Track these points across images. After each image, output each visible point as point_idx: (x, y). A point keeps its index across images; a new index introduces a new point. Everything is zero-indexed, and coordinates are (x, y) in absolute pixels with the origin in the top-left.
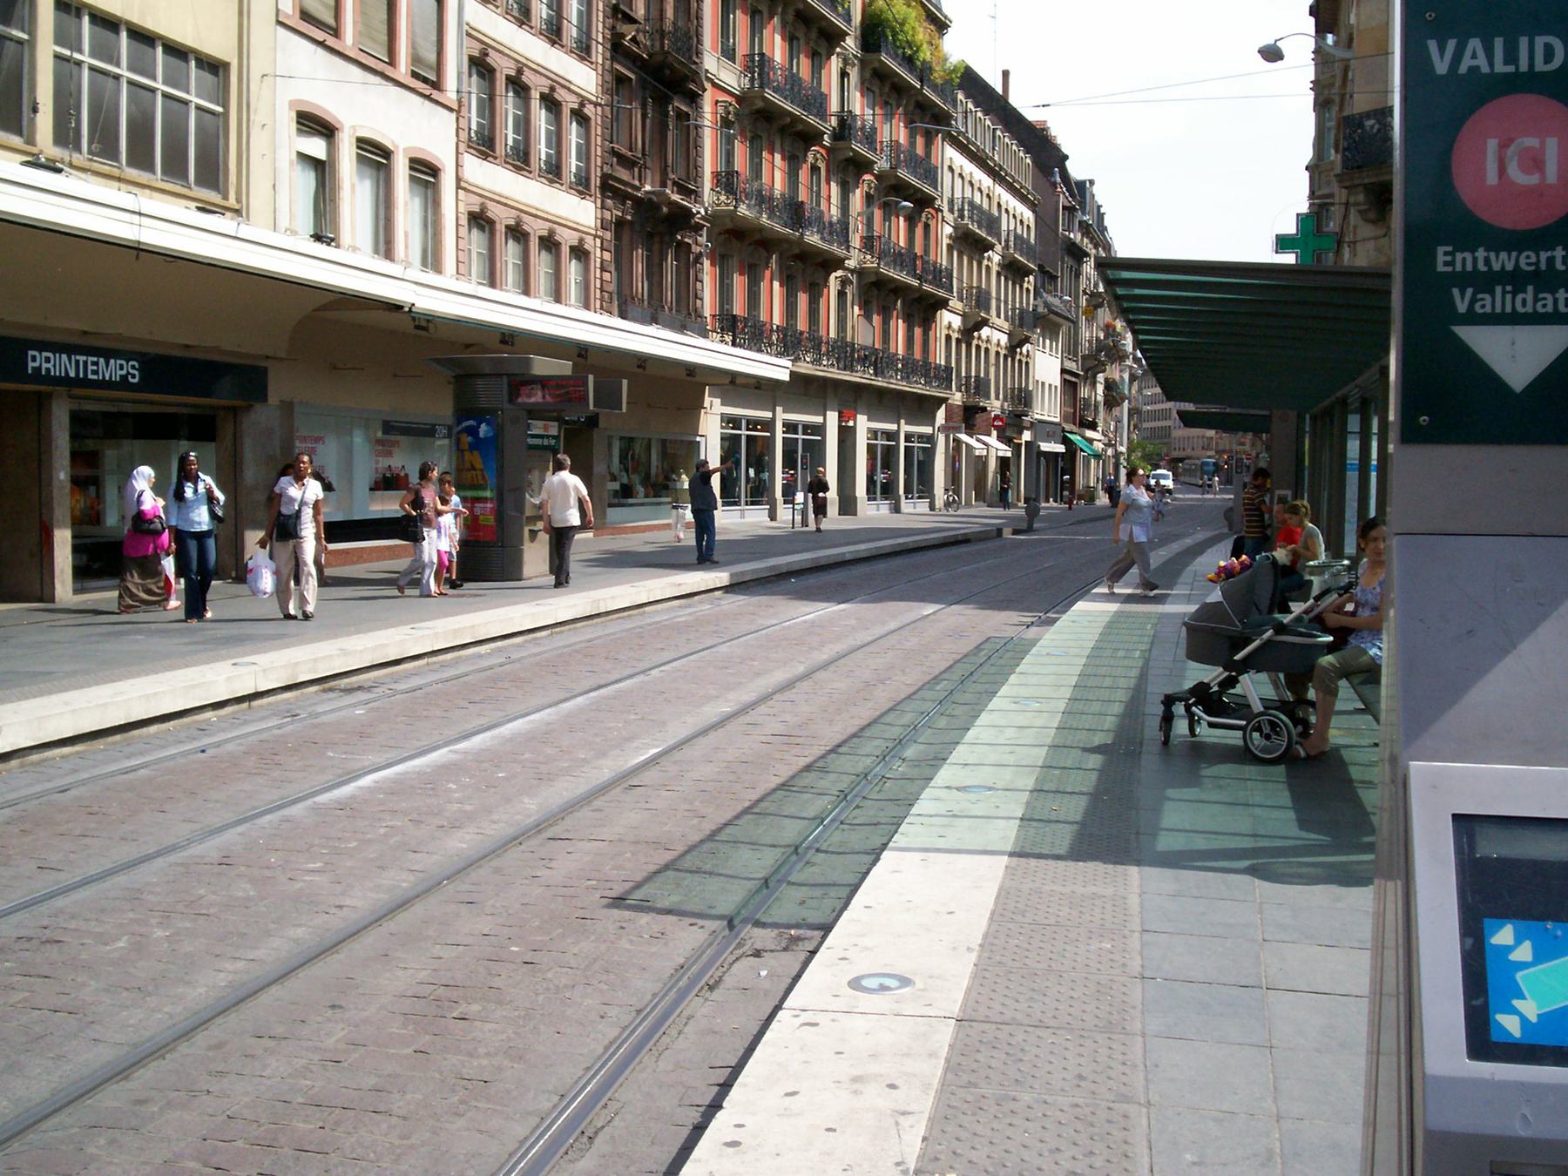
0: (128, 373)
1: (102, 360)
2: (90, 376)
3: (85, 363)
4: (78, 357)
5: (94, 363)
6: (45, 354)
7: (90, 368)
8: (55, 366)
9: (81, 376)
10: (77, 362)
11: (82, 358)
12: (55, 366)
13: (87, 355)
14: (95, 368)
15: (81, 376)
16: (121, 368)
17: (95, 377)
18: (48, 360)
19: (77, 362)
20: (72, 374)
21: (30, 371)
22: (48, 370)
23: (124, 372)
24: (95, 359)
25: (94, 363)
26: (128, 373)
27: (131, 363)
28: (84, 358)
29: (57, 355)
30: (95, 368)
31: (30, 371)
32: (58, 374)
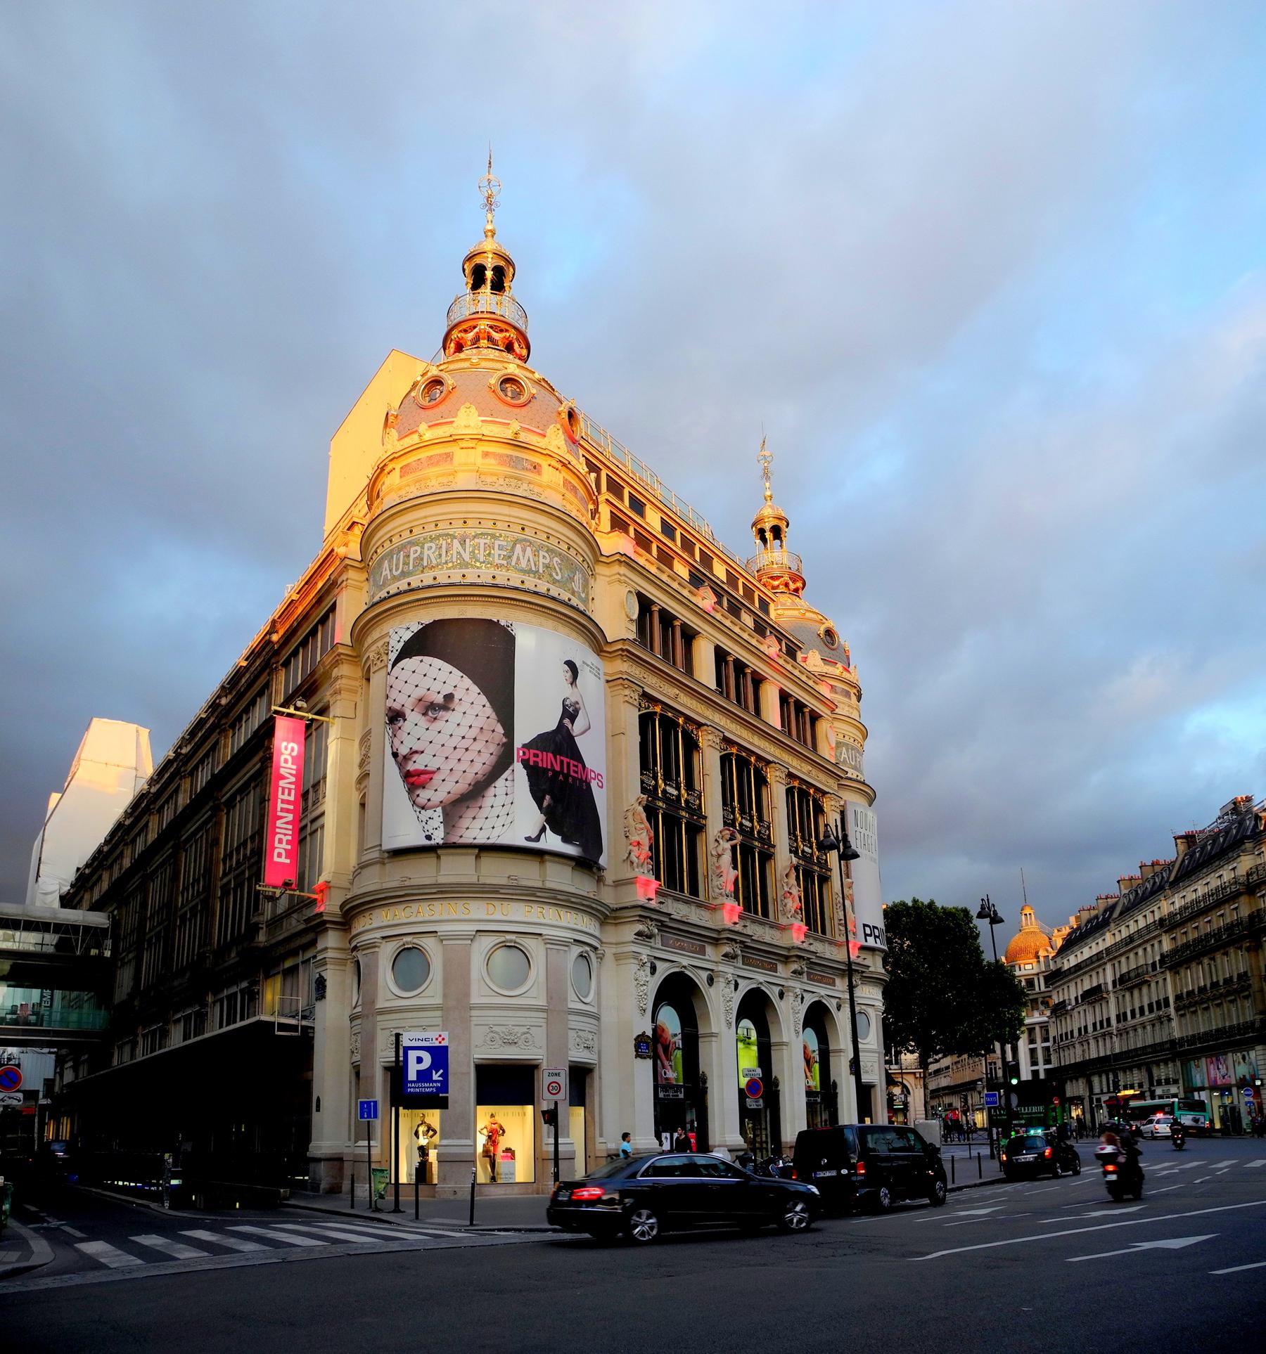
0: (290, 754)
1: (282, 783)
2: (292, 798)
3: (283, 801)
4: (279, 809)
5: (283, 793)
6: (276, 844)
7: (286, 797)
8: (285, 835)
9: (291, 807)
10: (283, 810)
11: (280, 805)
12: (285, 835)
13: (277, 797)
14: (286, 791)
15: (291, 807)
16: (286, 761)
17: (293, 792)
18: (280, 841)
19: (283, 810)
20: (290, 817)
21: (288, 861)
22: (288, 842)
23: (289, 758)
24: (280, 789)
25: (283, 793)
26: (290, 754)
27: (283, 750)
28: (279, 801)
29: (277, 830)
30: (286, 791)
31: (288, 861)
32: (290, 832)
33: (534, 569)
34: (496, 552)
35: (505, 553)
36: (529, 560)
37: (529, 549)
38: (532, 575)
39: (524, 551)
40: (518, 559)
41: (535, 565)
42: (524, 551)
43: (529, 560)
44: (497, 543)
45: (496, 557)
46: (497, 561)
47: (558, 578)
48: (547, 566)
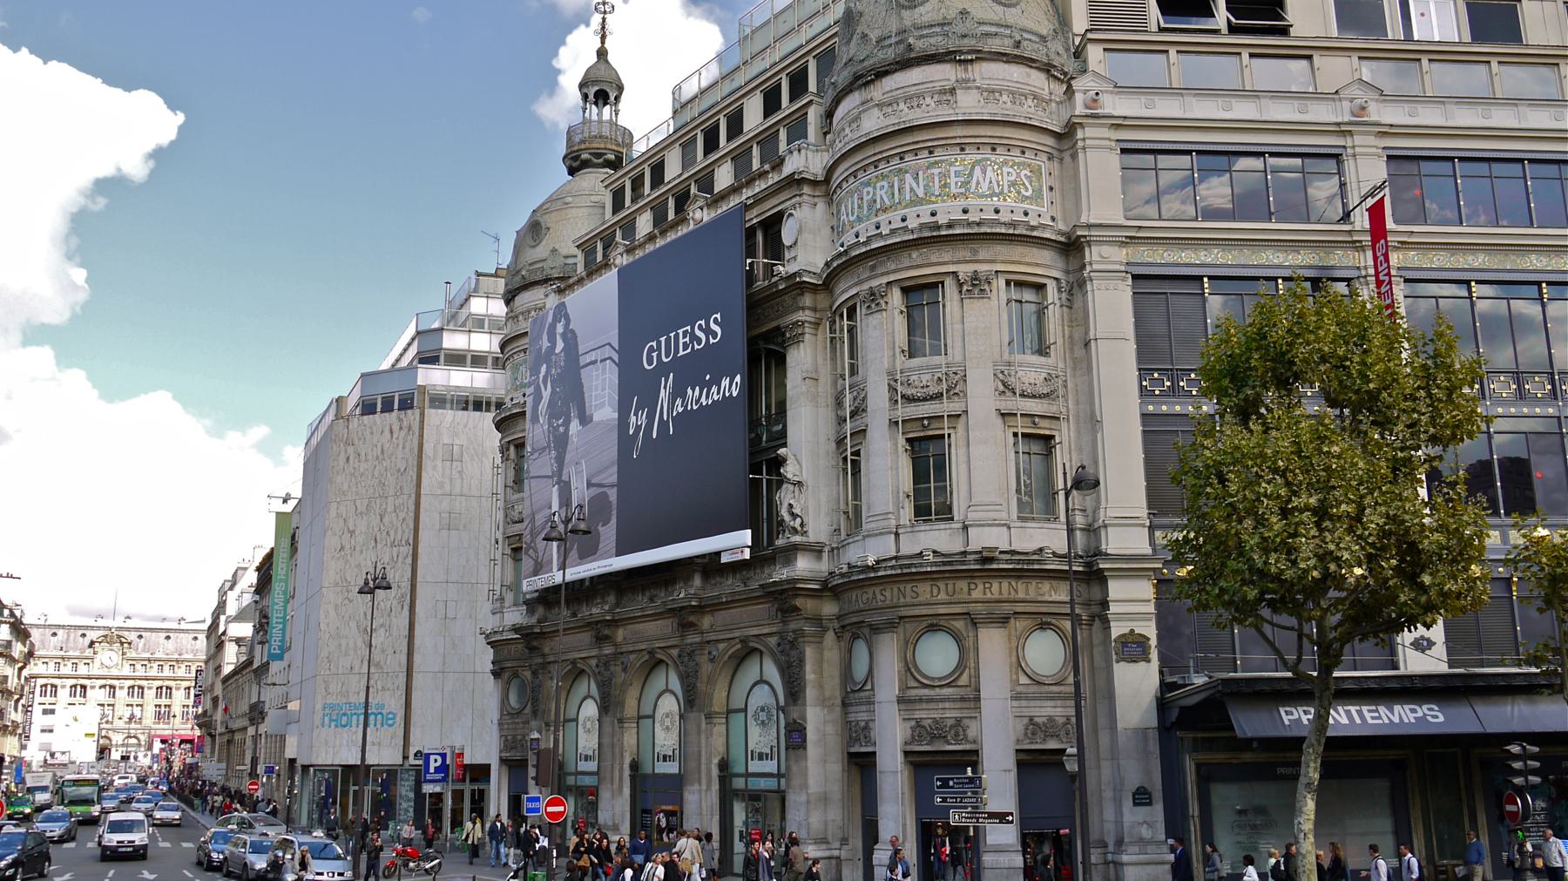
33: (997, 191)
34: (952, 180)
35: (963, 179)
36: (991, 182)
37: (989, 168)
38: (995, 199)
39: (984, 172)
40: (978, 183)
41: (999, 185)
42: (984, 172)
43: (991, 182)
44: (953, 169)
45: (953, 186)
46: (954, 190)
47: (1028, 194)
48: (1013, 184)
